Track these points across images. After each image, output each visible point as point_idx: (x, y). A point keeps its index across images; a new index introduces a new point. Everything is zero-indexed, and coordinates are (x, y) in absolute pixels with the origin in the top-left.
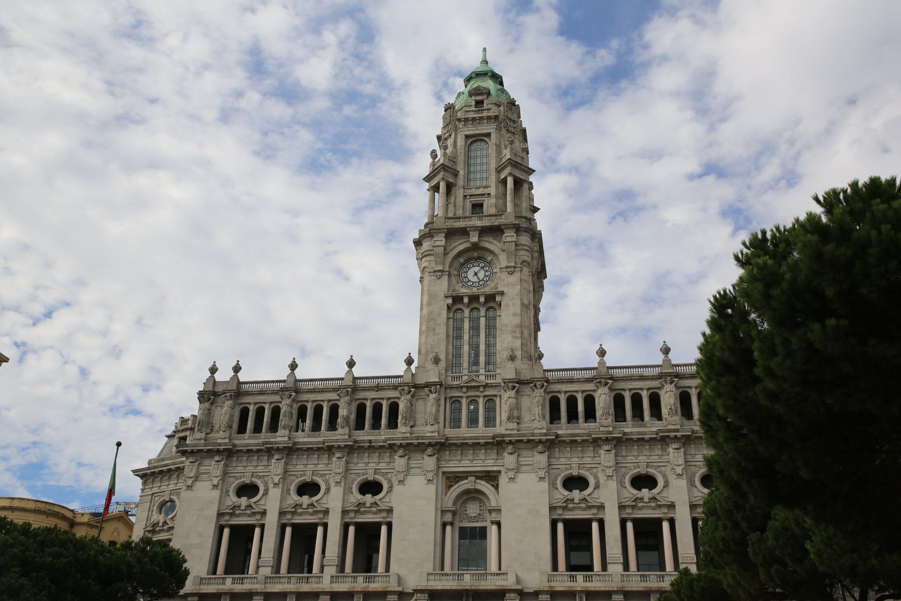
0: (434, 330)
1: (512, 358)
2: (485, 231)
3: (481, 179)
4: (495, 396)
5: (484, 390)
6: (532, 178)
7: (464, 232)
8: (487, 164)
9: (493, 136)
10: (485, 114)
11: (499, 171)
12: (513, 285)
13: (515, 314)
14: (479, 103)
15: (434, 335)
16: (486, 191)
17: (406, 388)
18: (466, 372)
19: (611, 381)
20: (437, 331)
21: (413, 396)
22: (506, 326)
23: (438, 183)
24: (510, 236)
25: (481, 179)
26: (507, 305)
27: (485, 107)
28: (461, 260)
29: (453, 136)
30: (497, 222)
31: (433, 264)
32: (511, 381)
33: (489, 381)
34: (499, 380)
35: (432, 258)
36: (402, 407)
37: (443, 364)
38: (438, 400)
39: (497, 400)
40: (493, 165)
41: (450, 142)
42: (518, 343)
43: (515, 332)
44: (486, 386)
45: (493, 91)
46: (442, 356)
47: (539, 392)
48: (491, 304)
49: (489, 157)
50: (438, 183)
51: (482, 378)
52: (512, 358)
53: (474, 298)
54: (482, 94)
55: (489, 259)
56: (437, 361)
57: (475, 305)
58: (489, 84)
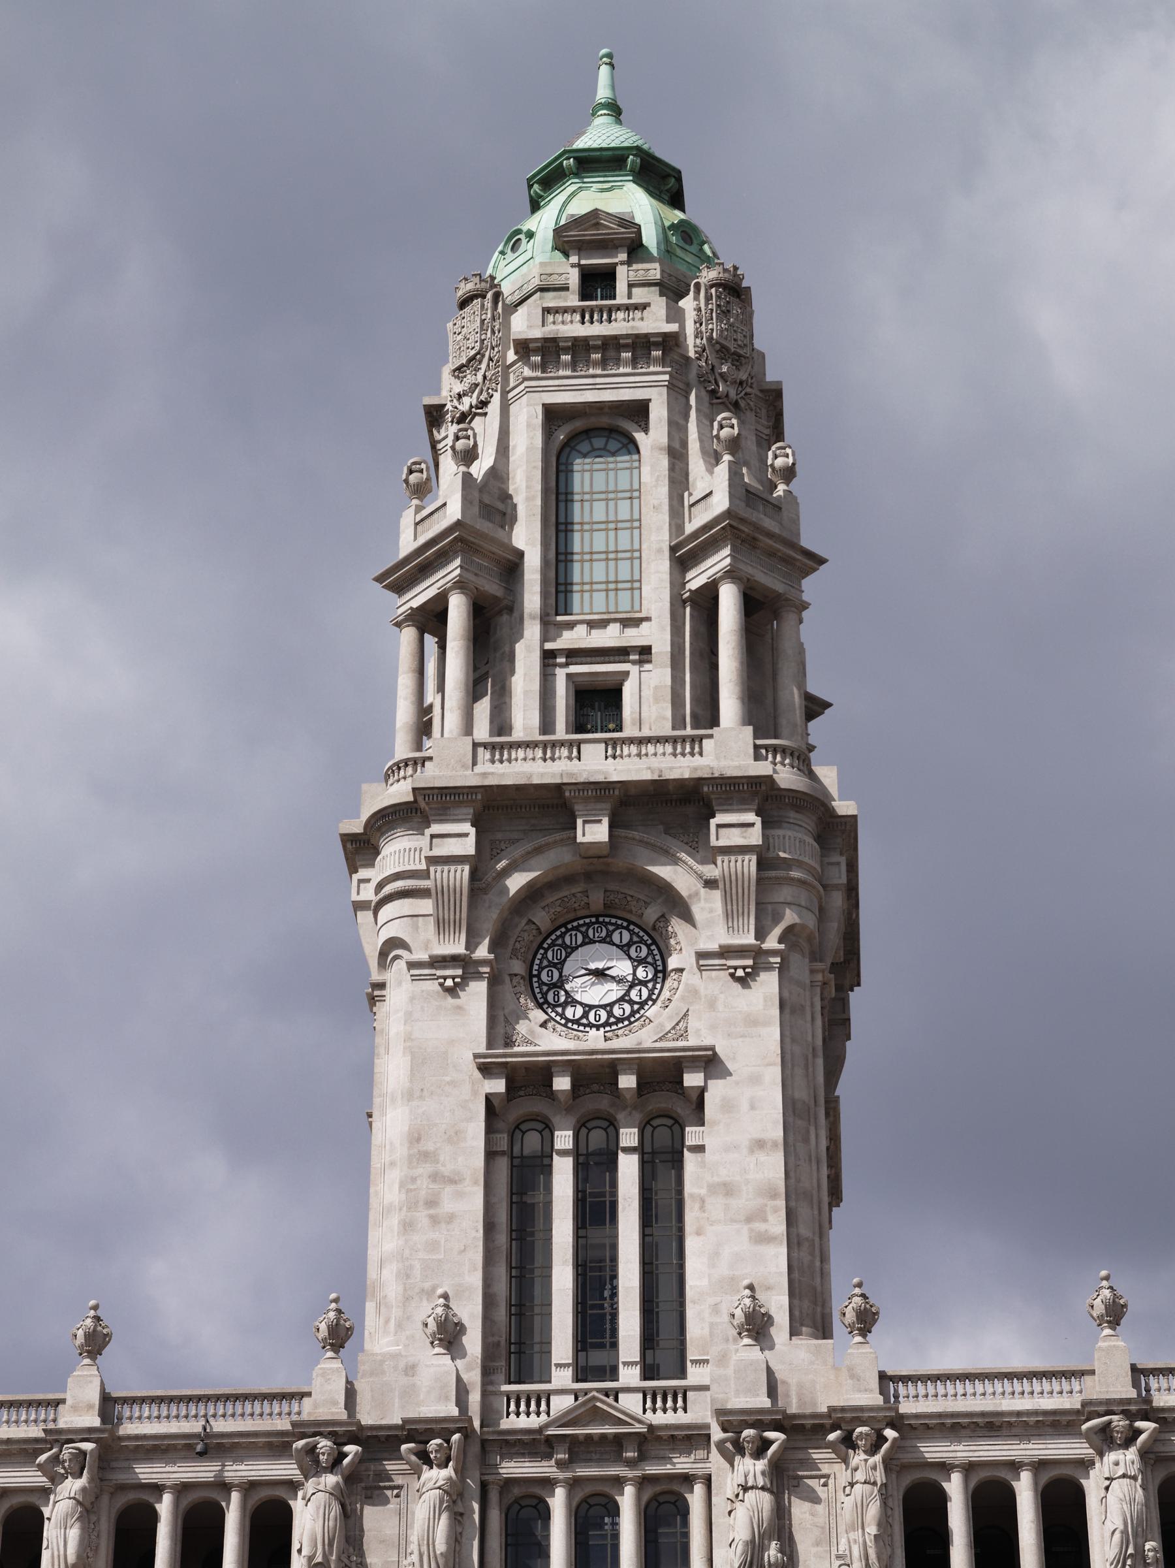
0: (432, 1203)
1: (756, 1326)
3: (612, 586)
4: (687, 1480)
5: (642, 1458)
6: (811, 587)
8: (635, 524)
9: (659, 413)
10: (620, 326)
11: (684, 558)
12: (752, 1021)
13: (759, 1144)
14: (597, 282)
15: (435, 1220)
16: (634, 637)
17: (324, 1444)
18: (562, 1378)
19: (1147, 1426)
20: (448, 1205)
21: (351, 1479)
22: (728, 1189)
23: (441, 601)
24: (737, 828)
25: (612, 586)
26: (728, 1106)
27: (621, 298)
28: (542, 918)
29: (494, 407)
30: (679, 767)
31: (428, 928)
32: (760, 1421)
33: (659, 1418)
34: (699, 1412)
35: (426, 906)
36: (310, 1520)
37: (473, 1342)
38: (453, 1498)
39: (696, 1499)
40: (657, 538)
41: (486, 429)
42: (773, 1264)
43: (755, 1216)
44: (653, 1442)
45: (650, 238)
46: (470, 1312)
47: (866, 1465)
48: (660, 1101)
49: (655, 505)
50: (441, 601)
51: (631, 1403)
52: (756, 1326)
53: (594, 1076)
54: (605, 245)
55: (651, 914)
56: (448, 1335)
57: (603, 1103)
58: (632, 201)
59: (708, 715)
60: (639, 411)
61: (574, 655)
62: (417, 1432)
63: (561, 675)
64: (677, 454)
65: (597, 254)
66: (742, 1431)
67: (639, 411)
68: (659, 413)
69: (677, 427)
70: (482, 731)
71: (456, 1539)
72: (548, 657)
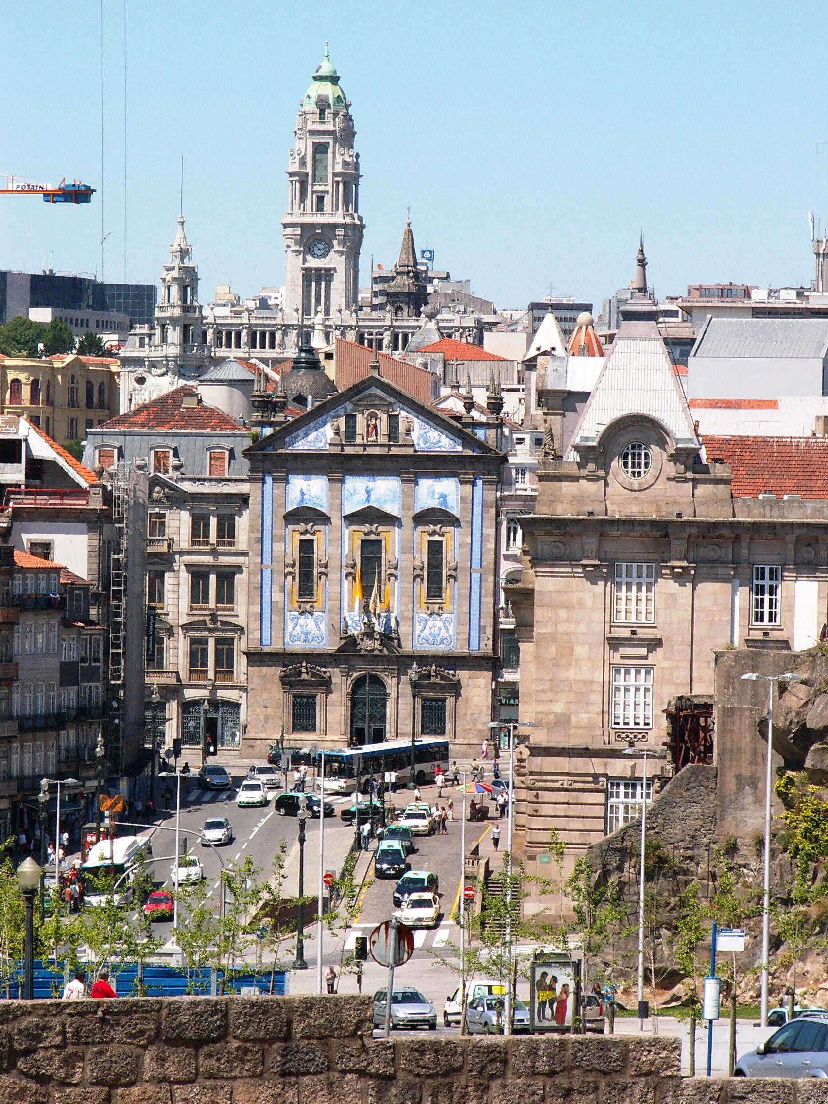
2: (323, 226)
7: (313, 226)
9: (331, 144)
11: (335, 175)
36: (278, 336)
37: (300, 312)
38: (298, 335)
45: (331, 102)
52: (340, 311)
56: (297, 310)
58: (328, 90)
59: (337, 209)
60: (328, 143)
61: (317, 192)
62: (293, 325)
63: (314, 196)
64: (334, 153)
65: (322, 105)
66: (337, 327)
67: (328, 143)
68: (331, 144)
69: (334, 147)
70: (302, 211)
71: (298, 341)
72: (313, 192)
